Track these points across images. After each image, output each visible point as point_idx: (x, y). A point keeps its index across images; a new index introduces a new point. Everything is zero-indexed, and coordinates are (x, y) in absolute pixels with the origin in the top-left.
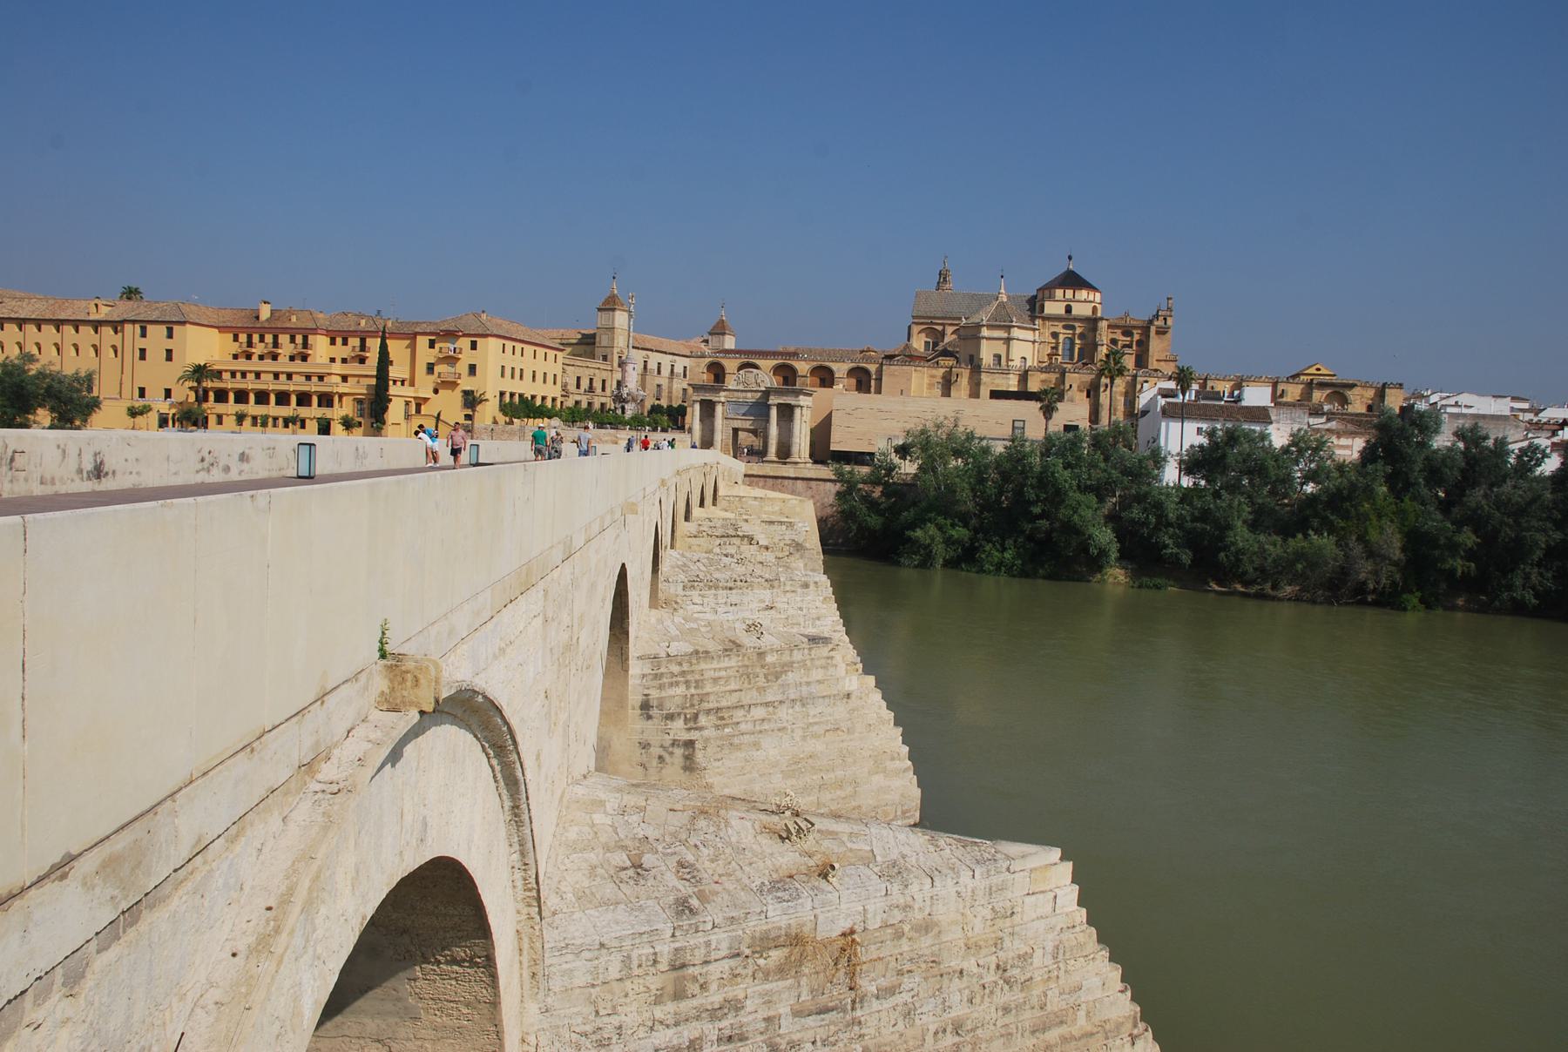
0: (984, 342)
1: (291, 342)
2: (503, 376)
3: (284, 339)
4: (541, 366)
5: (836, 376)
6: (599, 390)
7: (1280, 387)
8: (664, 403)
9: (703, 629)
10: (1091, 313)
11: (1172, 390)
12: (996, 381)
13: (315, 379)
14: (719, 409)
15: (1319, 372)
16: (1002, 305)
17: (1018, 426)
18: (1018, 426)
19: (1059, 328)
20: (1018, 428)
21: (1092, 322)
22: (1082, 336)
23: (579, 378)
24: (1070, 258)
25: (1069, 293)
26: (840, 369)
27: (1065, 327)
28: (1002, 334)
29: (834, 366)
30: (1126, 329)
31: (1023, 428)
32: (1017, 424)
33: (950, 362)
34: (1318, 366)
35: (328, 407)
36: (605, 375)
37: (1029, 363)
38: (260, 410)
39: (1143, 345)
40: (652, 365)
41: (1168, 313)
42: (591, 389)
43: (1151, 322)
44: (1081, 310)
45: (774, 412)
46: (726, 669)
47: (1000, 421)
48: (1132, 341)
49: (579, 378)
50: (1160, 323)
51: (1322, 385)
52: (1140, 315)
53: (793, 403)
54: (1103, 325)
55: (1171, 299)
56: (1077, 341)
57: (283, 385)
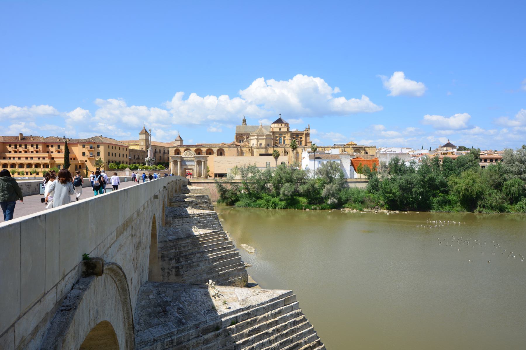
1: (32, 147)
2: (109, 155)
3: (29, 147)
4: (122, 152)
6: (141, 159)
8: (162, 161)
9: (180, 231)
12: (261, 151)
13: (41, 159)
14: (179, 163)
15: (352, 144)
17: (268, 164)
18: (268, 164)
20: (268, 164)
23: (135, 156)
24: (280, 115)
25: (280, 125)
26: (215, 150)
29: (214, 149)
32: (268, 163)
34: (352, 142)
35: (47, 167)
36: (143, 154)
38: (21, 170)
40: (158, 150)
41: (309, 129)
42: (139, 158)
46: (187, 243)
47: (263, 163)
49: (135, 156)
51: (353, 147)
52: (301, 130)
53: (202, 160)
57: (29, 161)
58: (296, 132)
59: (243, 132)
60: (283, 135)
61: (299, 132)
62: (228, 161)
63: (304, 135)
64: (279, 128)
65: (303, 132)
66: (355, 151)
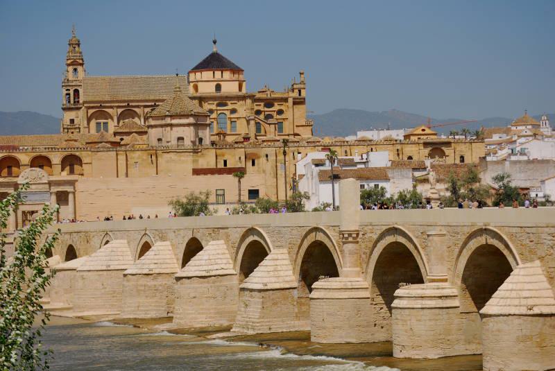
11: (321, 160)
15: (424, 133)
20: (221, 195)
22: (233, 111)
24: (215, 42)
25: (218, 74)
26: (56, 159)
27: (218, 105)
30: (268, 101)
31: (224, 195)
32: (219, 192)
34: (423, 128)
41: (302, 86)
51: (426, 144)
53: (69, 190)
55: (302, 74)
58: (263, 96)
59: (107, 98)
60: (230, 107)
62: (114, 190)
63: (291, 100)
64: (215, 83)
65: (285, 96)
66: (431, 155)
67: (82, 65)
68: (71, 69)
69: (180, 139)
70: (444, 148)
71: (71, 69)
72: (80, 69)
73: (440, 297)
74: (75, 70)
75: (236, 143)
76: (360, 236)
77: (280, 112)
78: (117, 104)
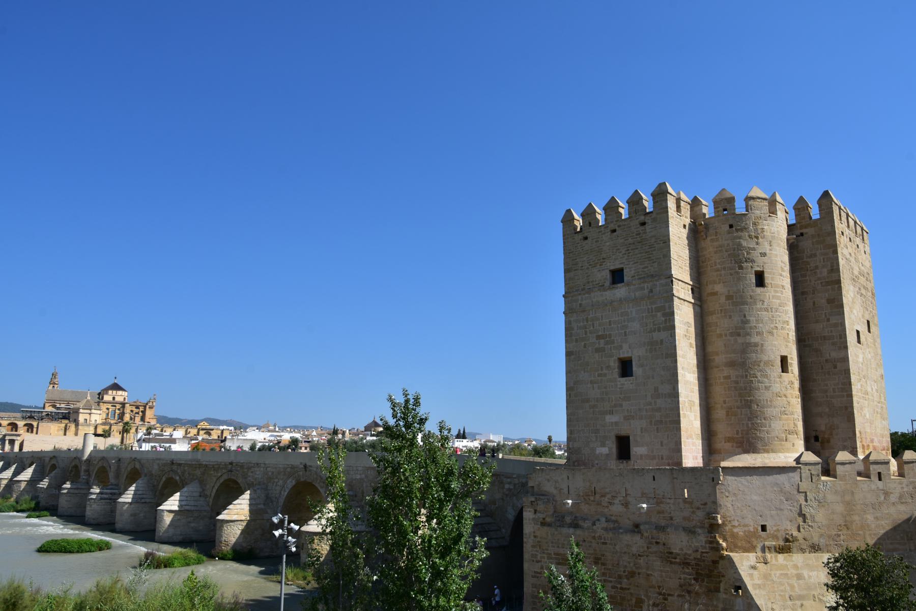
0: (80, 415)
5: (19, 426)
7: (189, 430)
10: (123, 400)
12: (85, 429)
16: (88, 401)
19: (109, 406)
21: (123, 405)
22: (119, 409)
24: (116, 378)
25: (114, 392)
27: (112, 406)
28: (88, 411)
33: (67, 421)
37: (98, 422)
39: (144, 412)
43: (147, 404)
44: (119, 399)
45: (7, 442)
48: (139, 411)
50: (150, 404)
51: (203, 429)
53: (15, 439)
54: (127, 405)
56: (117, 411)
58: (136, 404)
61: (140, 404)
62: (43, 440)
66: (205, 433)
67: (57, 384)
68: (52, 385)
69: (86, 420)
70: (211, 432)
71: (52, 385)
72: (56, 386)
73: (111, 494)
74: (53, 386)
75: (116, 423)
76: (91, 462)
77: (142, 412)
78: (62, 402)
